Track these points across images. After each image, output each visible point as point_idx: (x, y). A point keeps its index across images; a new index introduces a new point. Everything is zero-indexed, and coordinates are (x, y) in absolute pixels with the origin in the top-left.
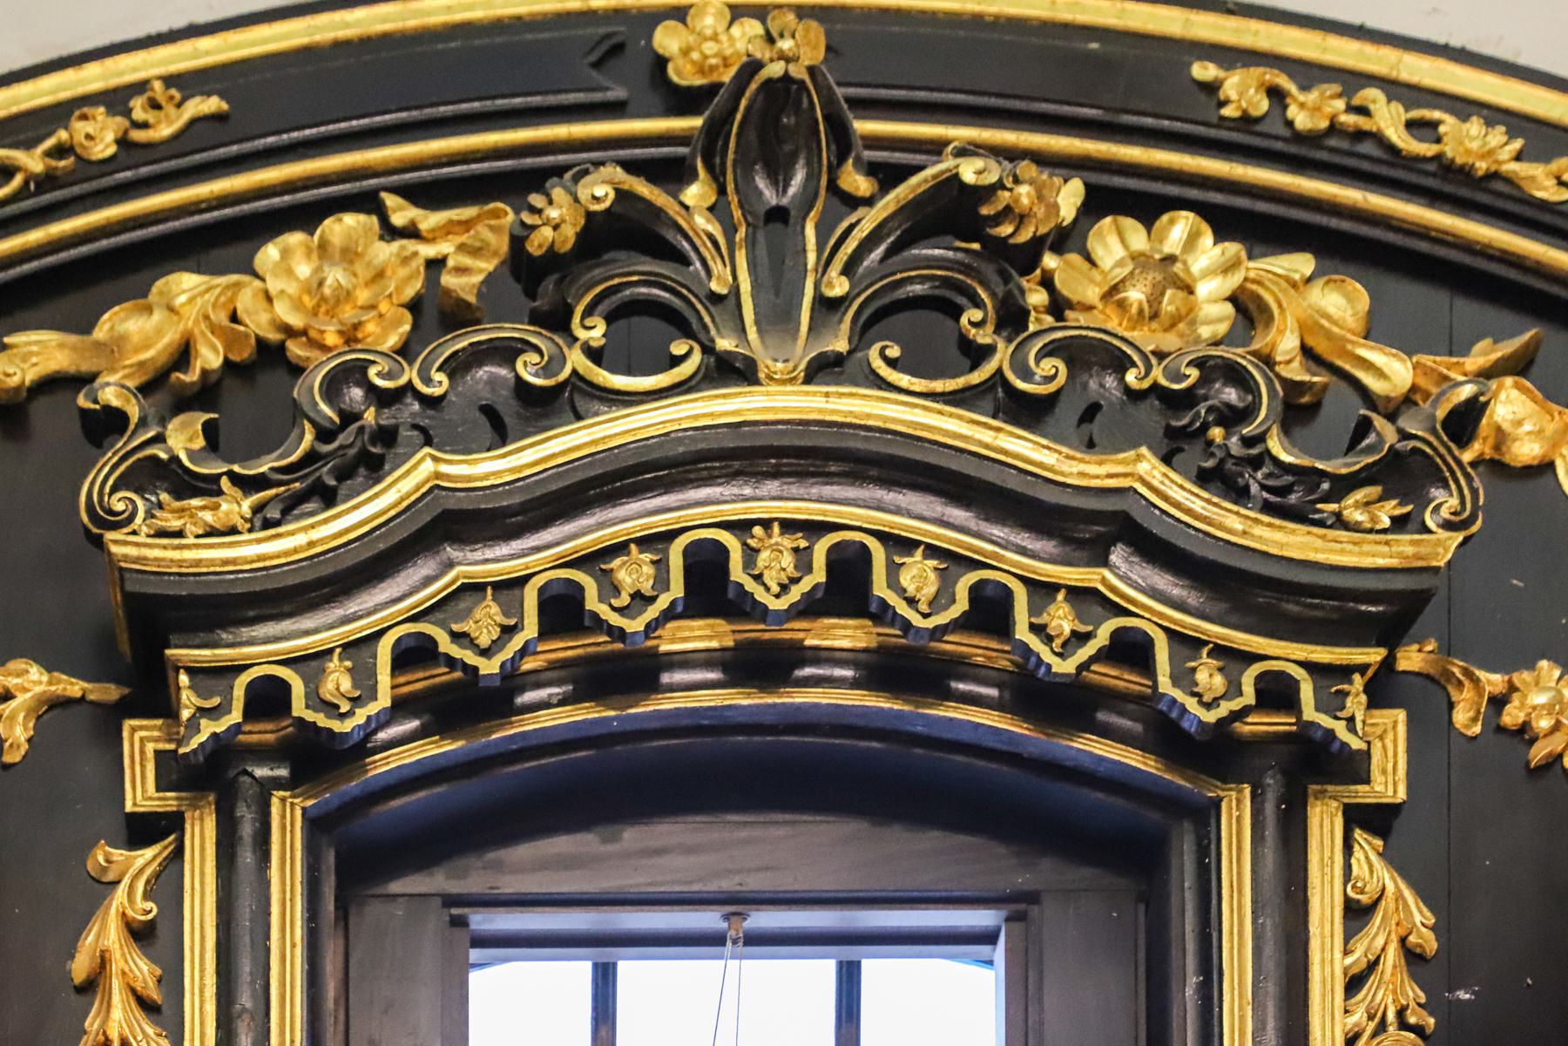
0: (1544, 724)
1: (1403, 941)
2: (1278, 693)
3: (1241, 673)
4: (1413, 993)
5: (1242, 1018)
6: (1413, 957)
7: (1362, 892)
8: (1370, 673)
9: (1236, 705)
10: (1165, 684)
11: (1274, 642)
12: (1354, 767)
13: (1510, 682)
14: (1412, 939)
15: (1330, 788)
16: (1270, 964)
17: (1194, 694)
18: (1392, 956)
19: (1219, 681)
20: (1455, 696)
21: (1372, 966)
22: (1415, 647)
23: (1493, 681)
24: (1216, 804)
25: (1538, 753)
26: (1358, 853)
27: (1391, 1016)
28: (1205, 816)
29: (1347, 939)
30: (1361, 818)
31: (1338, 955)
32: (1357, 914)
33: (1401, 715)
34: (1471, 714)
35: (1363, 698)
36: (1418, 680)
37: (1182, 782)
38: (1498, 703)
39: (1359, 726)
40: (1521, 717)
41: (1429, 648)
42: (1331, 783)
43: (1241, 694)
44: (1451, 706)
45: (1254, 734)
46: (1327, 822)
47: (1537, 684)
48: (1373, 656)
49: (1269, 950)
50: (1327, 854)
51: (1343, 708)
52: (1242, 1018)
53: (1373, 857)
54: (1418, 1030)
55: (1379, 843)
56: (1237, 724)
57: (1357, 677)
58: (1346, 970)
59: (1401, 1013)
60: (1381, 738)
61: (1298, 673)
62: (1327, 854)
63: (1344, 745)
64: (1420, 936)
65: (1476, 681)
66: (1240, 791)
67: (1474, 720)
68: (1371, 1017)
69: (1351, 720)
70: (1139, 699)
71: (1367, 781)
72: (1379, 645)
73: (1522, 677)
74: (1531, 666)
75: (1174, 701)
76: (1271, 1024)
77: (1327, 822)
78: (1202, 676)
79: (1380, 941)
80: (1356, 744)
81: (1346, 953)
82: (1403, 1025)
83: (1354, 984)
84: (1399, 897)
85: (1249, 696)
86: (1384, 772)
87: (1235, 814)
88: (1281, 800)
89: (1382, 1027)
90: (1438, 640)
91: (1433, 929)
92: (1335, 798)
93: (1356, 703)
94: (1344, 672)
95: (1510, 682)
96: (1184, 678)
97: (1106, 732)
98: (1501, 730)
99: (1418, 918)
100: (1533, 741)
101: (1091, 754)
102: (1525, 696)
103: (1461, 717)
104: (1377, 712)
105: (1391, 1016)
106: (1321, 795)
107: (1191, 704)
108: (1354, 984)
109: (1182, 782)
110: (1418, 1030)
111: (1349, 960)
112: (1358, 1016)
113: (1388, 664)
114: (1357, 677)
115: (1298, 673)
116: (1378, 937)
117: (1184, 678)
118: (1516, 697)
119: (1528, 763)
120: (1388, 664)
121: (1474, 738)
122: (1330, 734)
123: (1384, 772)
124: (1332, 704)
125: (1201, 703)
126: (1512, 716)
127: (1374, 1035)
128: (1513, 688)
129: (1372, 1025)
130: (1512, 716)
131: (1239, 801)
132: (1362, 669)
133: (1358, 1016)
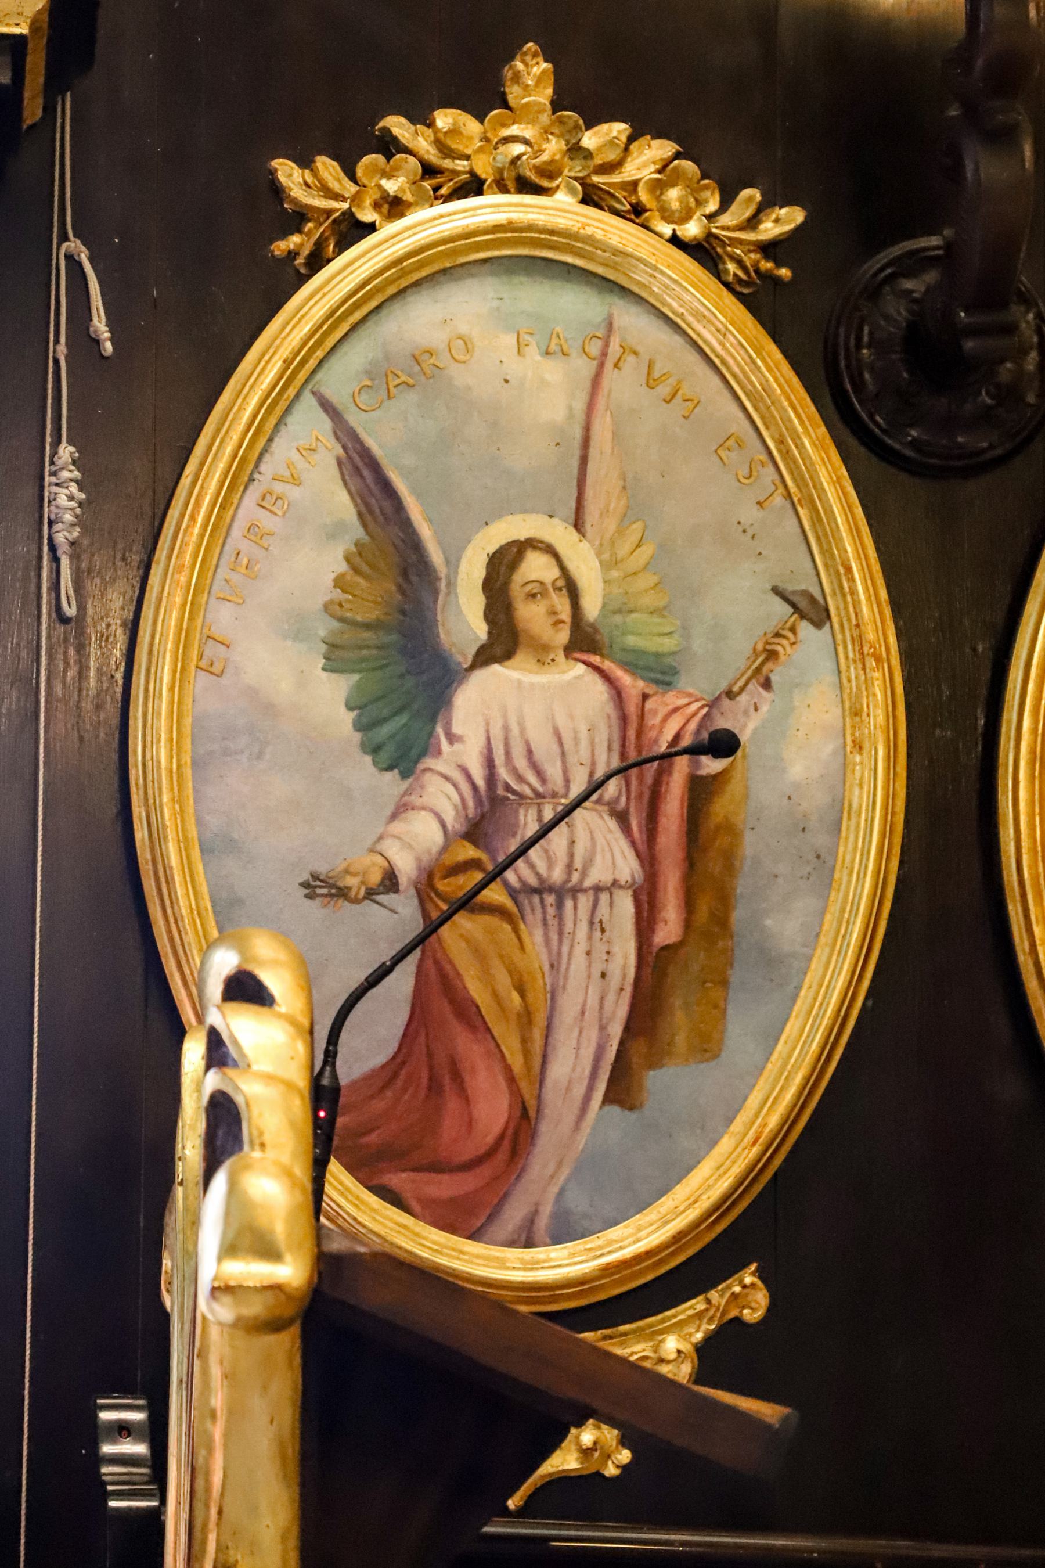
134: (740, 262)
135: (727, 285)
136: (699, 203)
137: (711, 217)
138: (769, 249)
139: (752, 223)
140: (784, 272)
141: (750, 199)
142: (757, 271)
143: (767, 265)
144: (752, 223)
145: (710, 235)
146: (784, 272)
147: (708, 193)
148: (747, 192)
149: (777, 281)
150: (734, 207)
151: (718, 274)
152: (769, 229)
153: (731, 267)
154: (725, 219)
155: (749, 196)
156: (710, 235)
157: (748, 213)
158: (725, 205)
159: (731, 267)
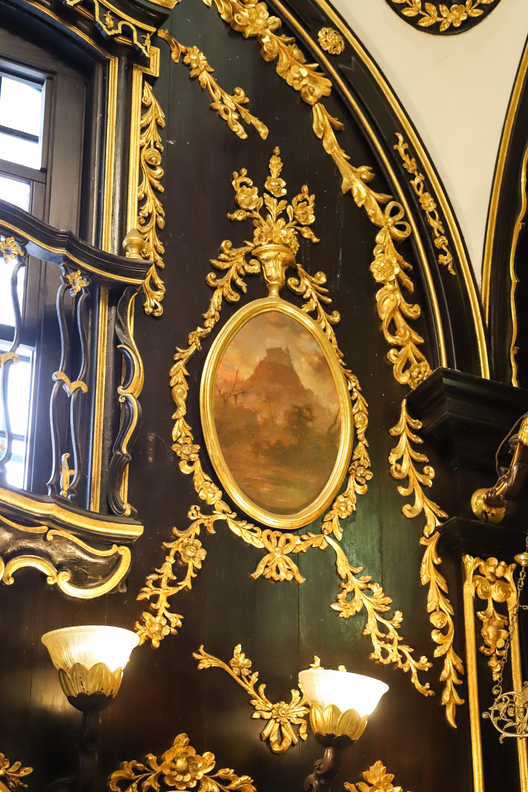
0: (194, 65)
1: (156, 120)
2: (127, 32)
3: (118, 22)
4: (158, 138)
5: (112, 131)
6: (159, 126)
7: (146, 102)
8: (152, 34)
9: (116, 32)
10: (97, 19)
11: (127, 16)
12: (145, 62)
13: (186, 50)
14: (159, 120)
15: (139, 66)
16: (120, 117)
17: (105, 25)
18: (153, 125)
19: (112, 22)
20: (172, 49)
21: (148, 125)
22: (163, 30)
23: (182, 48)
24: (109, 61)
25: (193, 73)
26: (145, 90)
27: (152, 144)
28: (106, 64)
29: (142, 115)
30: (148, 79)
31: (139, 119)
32: (145, 108)
33: (159, 50)
34: (176, 56)
35: (150, 42)
36: (163, 41)
37: (100, 51)
38: (183, 55)
39: (148, 50)
40: (189, 61)
41: (166, 32)
42: (141, 65)
43: (118, 29)
44: (171, 52)
45: (120, 43)
46: (138, 76)
47: (193, 52)
48: (153, 30)
49: (120, 112)
50: (138, 87)
51: (144, 43)
52: (112, 131)
53: (150, 92)
54: (159, 150)
55: (151, 88)
56: (116, 38)
57: (148, 34)
58: (141, 125)
59: (155, 143)
60: (153, 55)
61: (133, 28)
62: (138, 87)
63: (144, 54)
64: (161, 120)
65: (178, 46)
66: (115, 59)
67: (177, 58)
68: (147, 142)
69: (146, 47)
70: (89, 20)
71: (149, 67)
72: (155, 27)
73: (189, 49)
74: (192, 47)
75: (100, 25)
76: (120, 136)
77: (138, 76)
78: (107, 19)
79: (150, 119)
80: (147, 55)
81: (142, 119)
82: (155, 147)
83: (143, 130)
84: (156, 106)
85: (120, 31)
86: (153, 66)
87: (114, 66)
88: (126, 66)
89: (149, 146)
90: (169, 30)
91: (164, 119)
92: (140, 70)
93: (148, 42)
94: (145, 32)
95: (186, 50)
96: (103, 18)
97: (80, 28)
98: (183, 63)
99: (160, 115)
100: (191, 69)
101: (75, 33)
102: (190, 55)
103: (174, 56)
104: (152, 47)
105: (152, 144)
106: (137, 67)
107: (104, 27)
108: (143, 130)
109: (100, 51)
110: (159, 150)
111: (142, 122)
112: (143, 141)
113: (156, 33)
114: (148, 34)
115: (133, 28)
116: (149, 117)
117: (103, 18)
118: (188, 54)
119: (190, 76)
120: (156, 33)
121: (176, 63)
122: (141, 49)
123: (153, 66)
124: (142, 41)
125: (107, 28)
126: (186, 60)
127: (147, 148)
128: (187, 52)
129: (147, 145)
130: (186, 60)
131: (115, 62)
132: (150, 32)
133: (143, 141)
134: (14, 783)
135: (10, 789)
136: (4, 765)
137: (7, 769)
138: (22, 779)
139: (18, 772)
140: (26, 786)
141: (18, 765)
142: (18, 785)
143: (21, 784)
144: (18, 772)
145: (6, 774)
146: (26, 786)
147: (6, 763)
148: (17, 763)
149: (24, 788)
150: (13, 767)
151: (7, 785)
152: (23, 773)
153: (11, 784)
154: (11, 770)
155: (19, 763)
156: (6, 774)
157: (17, 769)
158: (10, 766)
159: (11, 784)
